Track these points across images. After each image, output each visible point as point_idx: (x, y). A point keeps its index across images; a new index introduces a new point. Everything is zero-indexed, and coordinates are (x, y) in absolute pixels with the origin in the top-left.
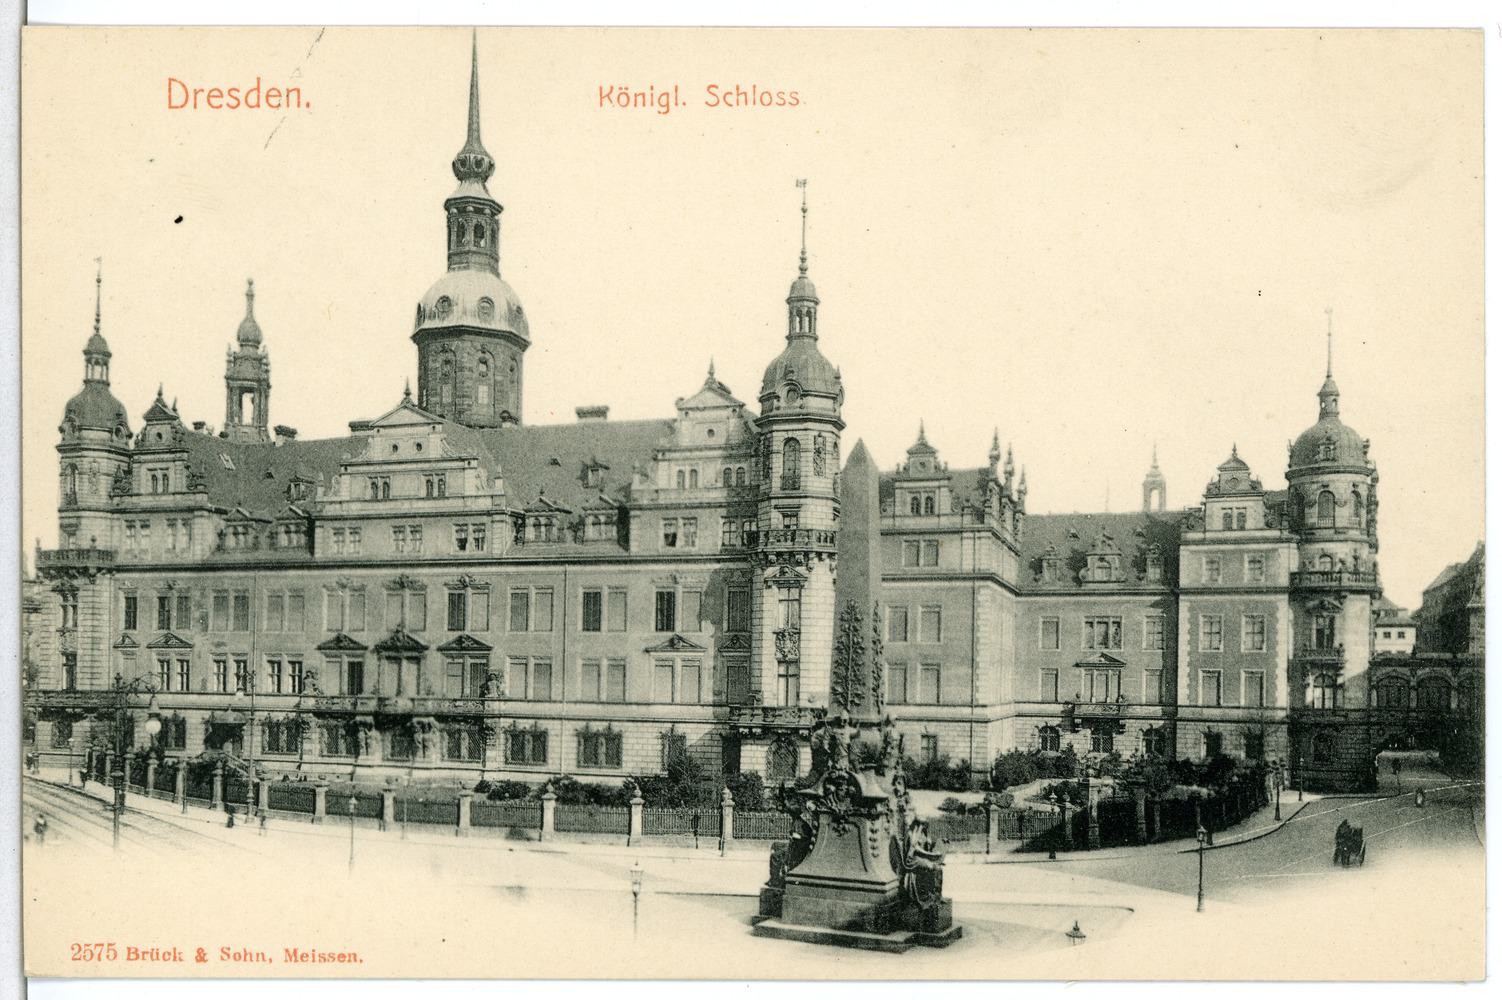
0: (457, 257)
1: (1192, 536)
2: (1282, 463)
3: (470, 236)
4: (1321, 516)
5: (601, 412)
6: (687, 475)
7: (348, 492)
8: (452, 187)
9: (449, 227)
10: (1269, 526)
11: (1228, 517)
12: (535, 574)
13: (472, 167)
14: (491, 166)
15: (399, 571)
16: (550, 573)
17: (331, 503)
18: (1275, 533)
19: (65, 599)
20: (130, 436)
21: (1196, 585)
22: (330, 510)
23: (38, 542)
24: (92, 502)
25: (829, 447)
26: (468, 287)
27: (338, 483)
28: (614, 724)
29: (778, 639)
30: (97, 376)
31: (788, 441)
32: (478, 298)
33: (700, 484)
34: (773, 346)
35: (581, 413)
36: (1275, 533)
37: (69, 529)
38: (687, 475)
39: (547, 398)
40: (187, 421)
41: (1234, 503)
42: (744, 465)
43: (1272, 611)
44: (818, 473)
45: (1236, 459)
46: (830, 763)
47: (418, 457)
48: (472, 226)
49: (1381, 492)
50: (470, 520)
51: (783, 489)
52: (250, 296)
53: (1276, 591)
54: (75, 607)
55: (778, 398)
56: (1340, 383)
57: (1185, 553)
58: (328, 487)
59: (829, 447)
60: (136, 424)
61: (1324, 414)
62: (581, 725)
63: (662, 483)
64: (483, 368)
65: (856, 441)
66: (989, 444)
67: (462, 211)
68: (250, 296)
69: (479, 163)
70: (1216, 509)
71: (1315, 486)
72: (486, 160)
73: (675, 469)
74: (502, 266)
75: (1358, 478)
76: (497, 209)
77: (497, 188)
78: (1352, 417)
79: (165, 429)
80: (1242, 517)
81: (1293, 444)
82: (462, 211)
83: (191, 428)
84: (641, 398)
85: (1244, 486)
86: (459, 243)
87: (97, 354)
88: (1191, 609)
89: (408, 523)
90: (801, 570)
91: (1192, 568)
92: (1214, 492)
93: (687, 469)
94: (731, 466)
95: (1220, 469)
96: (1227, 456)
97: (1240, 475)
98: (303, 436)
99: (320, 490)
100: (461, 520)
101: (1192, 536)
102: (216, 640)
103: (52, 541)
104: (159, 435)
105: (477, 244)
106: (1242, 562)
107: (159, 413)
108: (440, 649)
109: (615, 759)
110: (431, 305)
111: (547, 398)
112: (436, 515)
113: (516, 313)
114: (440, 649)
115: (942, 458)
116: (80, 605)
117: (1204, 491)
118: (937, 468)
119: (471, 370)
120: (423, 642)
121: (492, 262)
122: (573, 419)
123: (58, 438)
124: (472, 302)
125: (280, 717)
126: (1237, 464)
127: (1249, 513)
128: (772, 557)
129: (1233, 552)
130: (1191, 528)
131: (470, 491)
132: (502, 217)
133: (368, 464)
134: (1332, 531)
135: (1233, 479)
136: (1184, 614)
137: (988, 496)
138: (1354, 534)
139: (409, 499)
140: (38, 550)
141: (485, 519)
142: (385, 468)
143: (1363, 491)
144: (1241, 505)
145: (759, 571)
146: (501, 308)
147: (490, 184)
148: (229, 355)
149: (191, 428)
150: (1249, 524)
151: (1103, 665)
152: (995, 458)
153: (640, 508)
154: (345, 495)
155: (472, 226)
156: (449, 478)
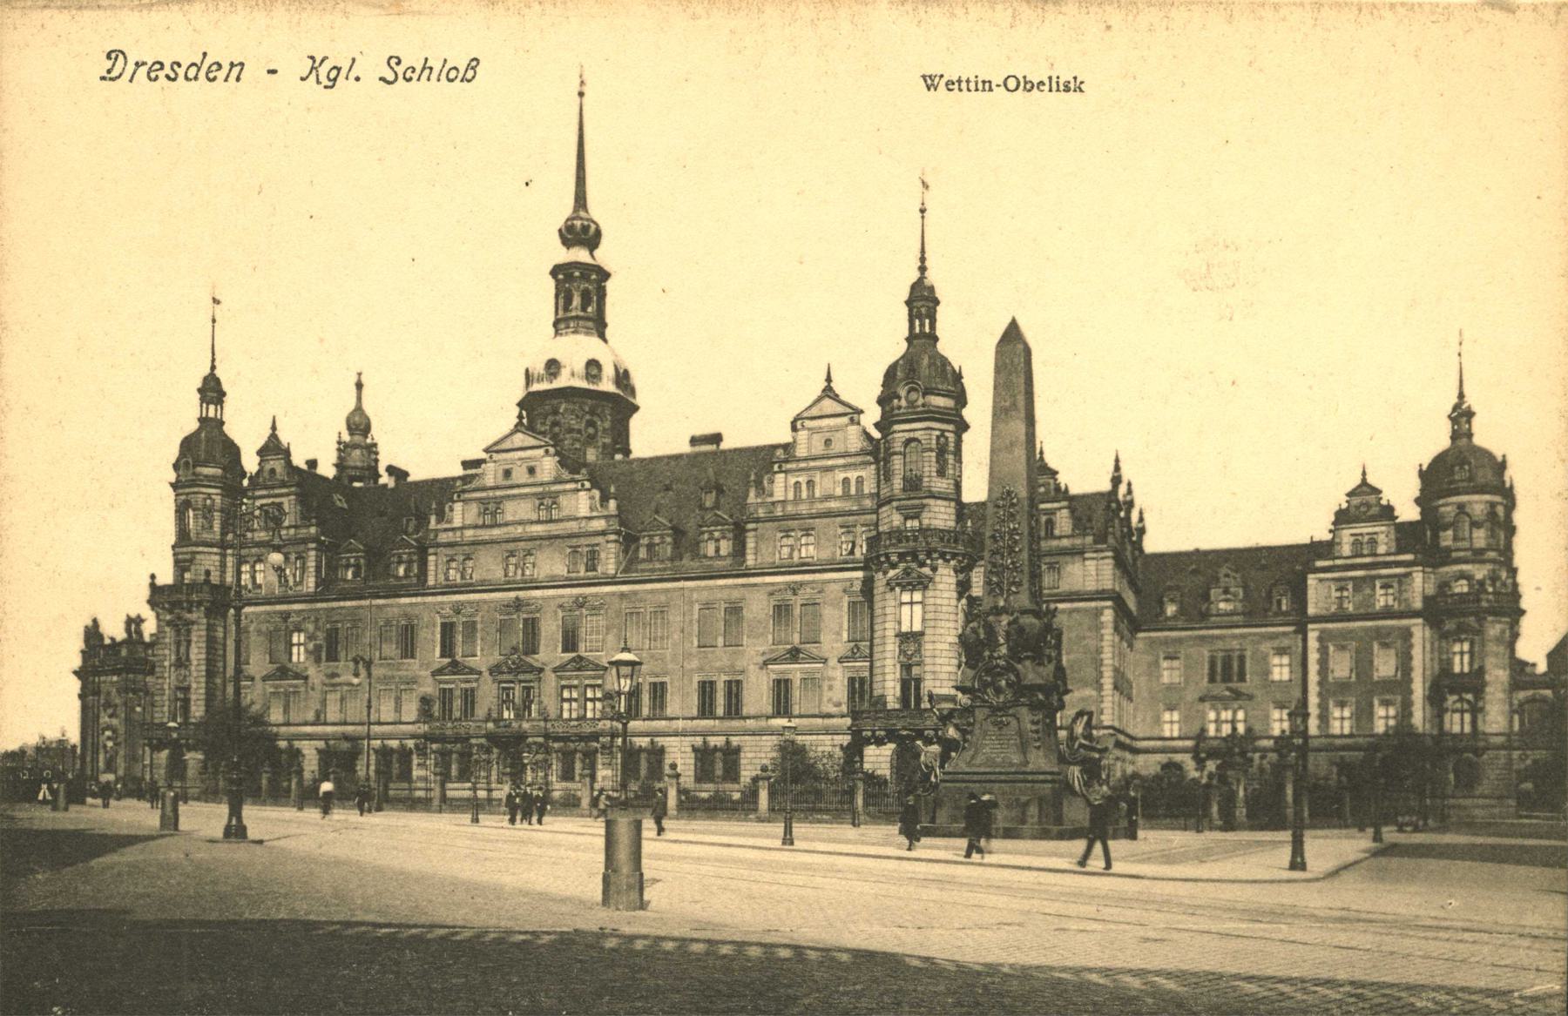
0: (561, 324)
1: (1319, 564)
2: (1413, 487)
3: (576, 301)
4: (1455, 539)
5: (716, 438)
6: (804, 487)
7: (460, 514)
8: (564, 255)
9: (557, 296)
10: (1400, 551)
11: (1357, 544)
12: (652, 591)
13: (580, 233)
14: (598, 233)
15: (512, 594)
16: (667, 590)
17: (446, 530)
18: (1409, 557)
19: (178, 632)
20: (243, 474)
21: (1324, 612)
22: (443, 538)
23: (153, 577)
24: (206, 536)
25: (951, 447)
26: (576, 350)
27: (452, 510)
28: (732, 739)
29: (902, 642)
30: (211, 414)
31: (908, 442)
32: (585, 360)
33: (817, 494)
34: (892, 345)
35: (694, 441)
36: (1409, 557)
37: (181, 566)
38: (804, 487)
39: (656, 434)
40: (299, 460)
41: (1365, 529)
42: (863, 473)
43: (1407, 634)
44: (941, 473)
45: (1364, 482)
46: (987, 653)
47: (531, 480)
48: (581, 294)
49: (1518, 517)
50: (583, 541)
51: (904, 490)
52: (359, 386)
53: (1415, 614)
54: (189, 642)
55: (899, 398)
56: (1472, 400)
57: (1312, 580)
58: (441, 516)
59: (951, 447)
60: (250, 463)
61: (1455, 436)
62: (699, 741)
63: (779, 494)
64: (591, 430)
65: (1009, 321)
66: (1111, 468)
67: (569, 278)
68: (359, 386)
69: (585, 229)
70: (1346, 536)
71: (1449, 509)
72: (593, 227)
73: (792, 480)
74: (608, 332)
75: (1497, 499)
76: (605, 275)
77: (604, 255)
78: (1484, 435)
79: (277, 465)
80: (1373, 542)
81: (1425, 468)
82: (569, 278)
83: (304, 467)
84: (752, 424)
85: (1375, 510)
86: (566, 309)
87: (212, 390)
88: (1320, 639)
89: (519, 548)
90: (926, 571)
91: (1319, 593)
92: (1343, 518)
93: (803, 479)
94: (849, 475)
95: (1348, 495)
96: (1356, 481)
97: (1372, 499)
98: (416, 475)
99: (433, 519)
100: (574, 542)
101: (1319, 564)
102: (329, 671)
103: (166, 577)
104: (273, 471)
105: (584, 309)
106: (1373, 588)
107: (273, 448)
108: (555, 670)
109: (732, 773)
110: (539, 367)
111: (656, 434)
112: (550, 538)
113: (623, 378)
114: (555, 670)
115: (1063, 479)
116: (194, 639)
117: (1333, 518)
118: (1058, 488)
119: (579, 431)
120: (536, 664)
121: (599, 326)
122: (685, 448)
123: (172, 477)
124: (580, 367)
125: (394, 744)
126: (1365, 489)
127: (1382, 538)
128: (894, 558)
129: (1363, 579)
130: (1321, 557)
131: (584, 510)
132: (610, 285)
133: (484, 489)
134: (1469, 554)
135: (1364, 504)
136: (1313, 644)
137: (1109, 517)
138: (1492, 554)
139: (520, 523)
140: (153, 586)
141: (600, 539)
142: (498, 493)
143: (1500, 510)
144: (1370, 530)
145: (880, 575)
146: (608, 371)
147: (597, 253)
148: (339, 443)
149: (304, 467)
150: (1382, 549)
151: (1227, 698)
152: (1116, 481)
153: (757, 520)
154: (457, 522)
155: (581, 294)
156: (563, 500)
